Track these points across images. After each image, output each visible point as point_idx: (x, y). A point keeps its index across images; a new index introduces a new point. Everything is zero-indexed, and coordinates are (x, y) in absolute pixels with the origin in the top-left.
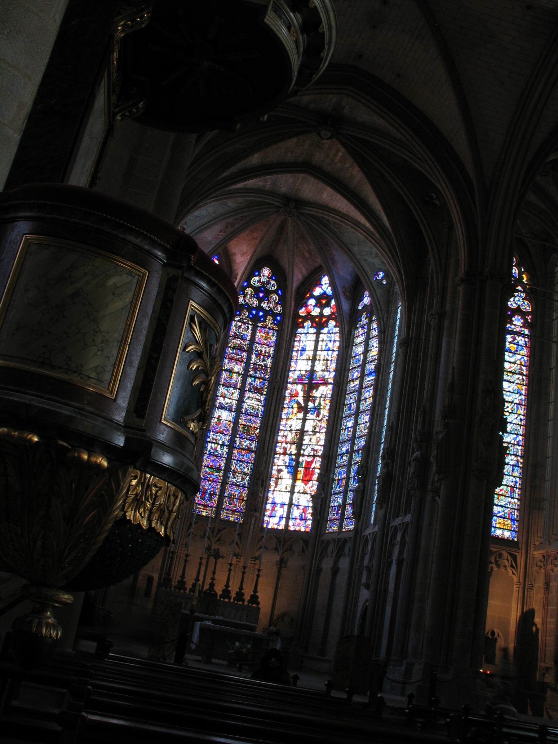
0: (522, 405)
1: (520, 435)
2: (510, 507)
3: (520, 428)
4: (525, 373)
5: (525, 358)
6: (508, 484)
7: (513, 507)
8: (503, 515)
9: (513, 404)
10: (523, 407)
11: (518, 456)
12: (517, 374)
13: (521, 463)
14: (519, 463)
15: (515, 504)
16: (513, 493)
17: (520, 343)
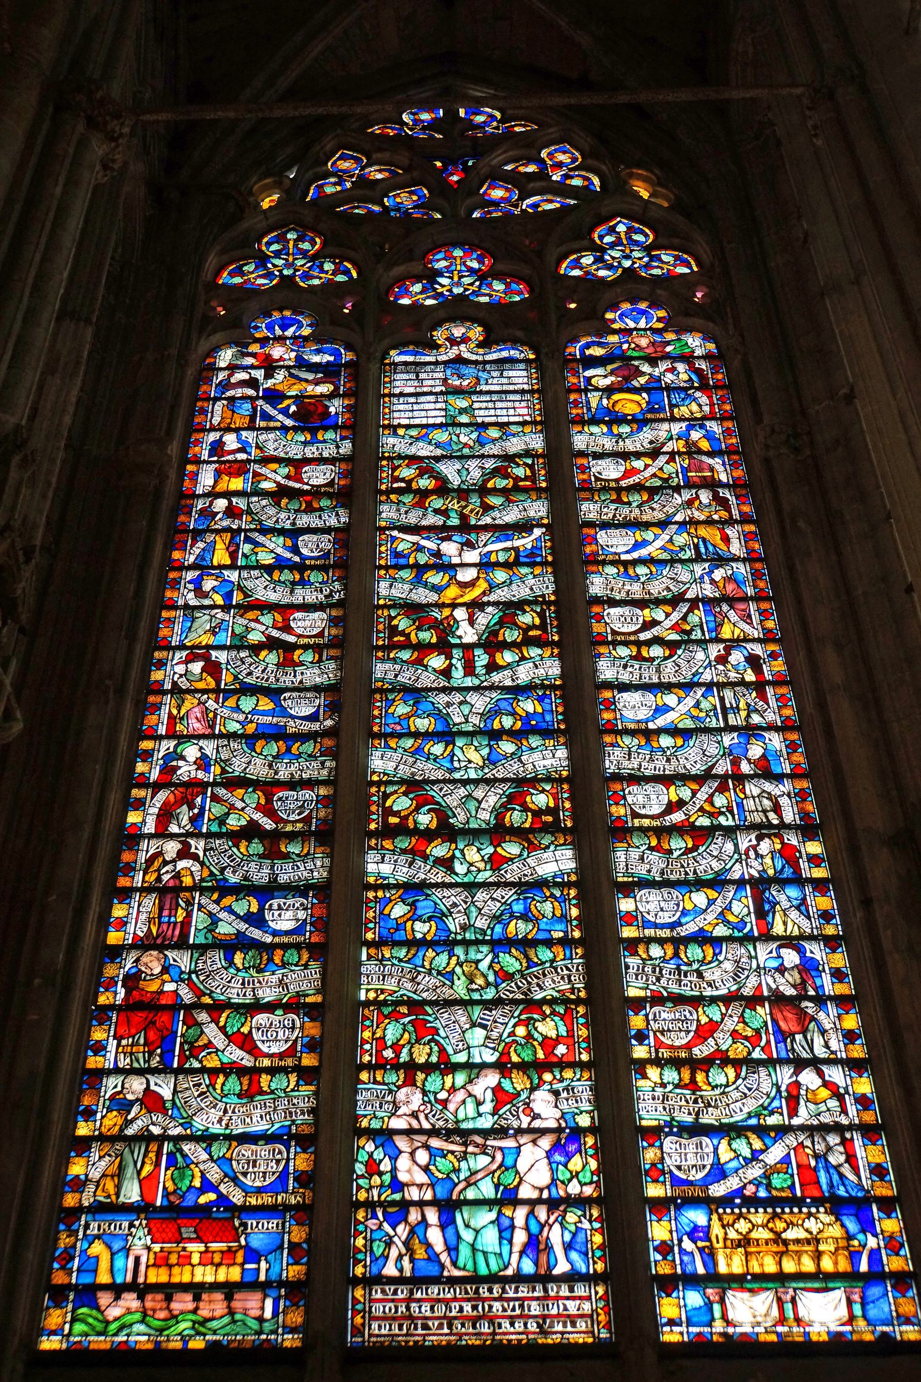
0: (745, 599)
1: (771, 727)
2: (796, 1121)
3: (763, 697)
4: (723, 478)
5: (714, 427)
6: (747, 991)
7: (826, 1119)
8: (756, 1183)
9: (684, 608)
10: (753, 607)
11: (783, 826)
12: (677, 489)
13: (814, 860)
14: (803, 864)
15: (840, 1098)
16: (804, 1032)
17: (669, 378)
